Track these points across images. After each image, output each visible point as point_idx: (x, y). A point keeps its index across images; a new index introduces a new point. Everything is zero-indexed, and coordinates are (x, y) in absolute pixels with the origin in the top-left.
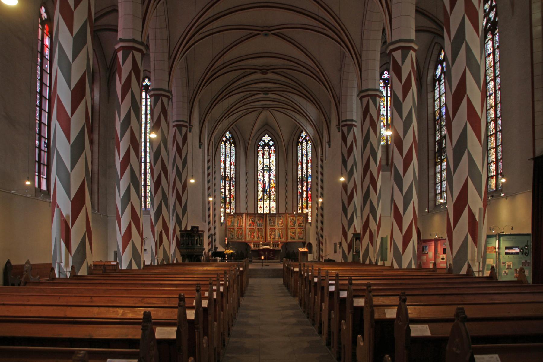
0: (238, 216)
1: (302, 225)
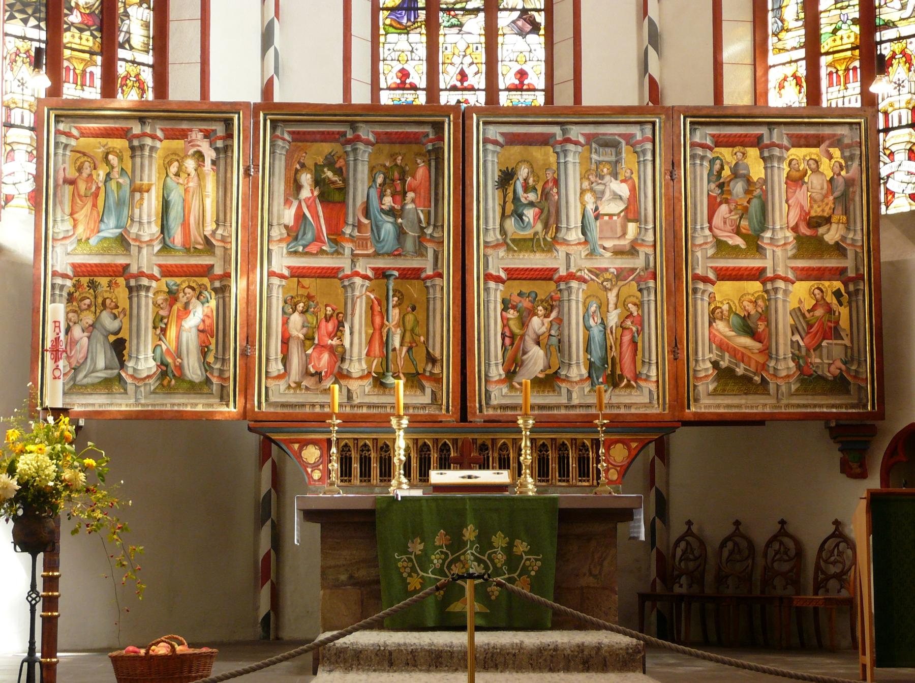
0: (171, 135)
1: (832, 235)
